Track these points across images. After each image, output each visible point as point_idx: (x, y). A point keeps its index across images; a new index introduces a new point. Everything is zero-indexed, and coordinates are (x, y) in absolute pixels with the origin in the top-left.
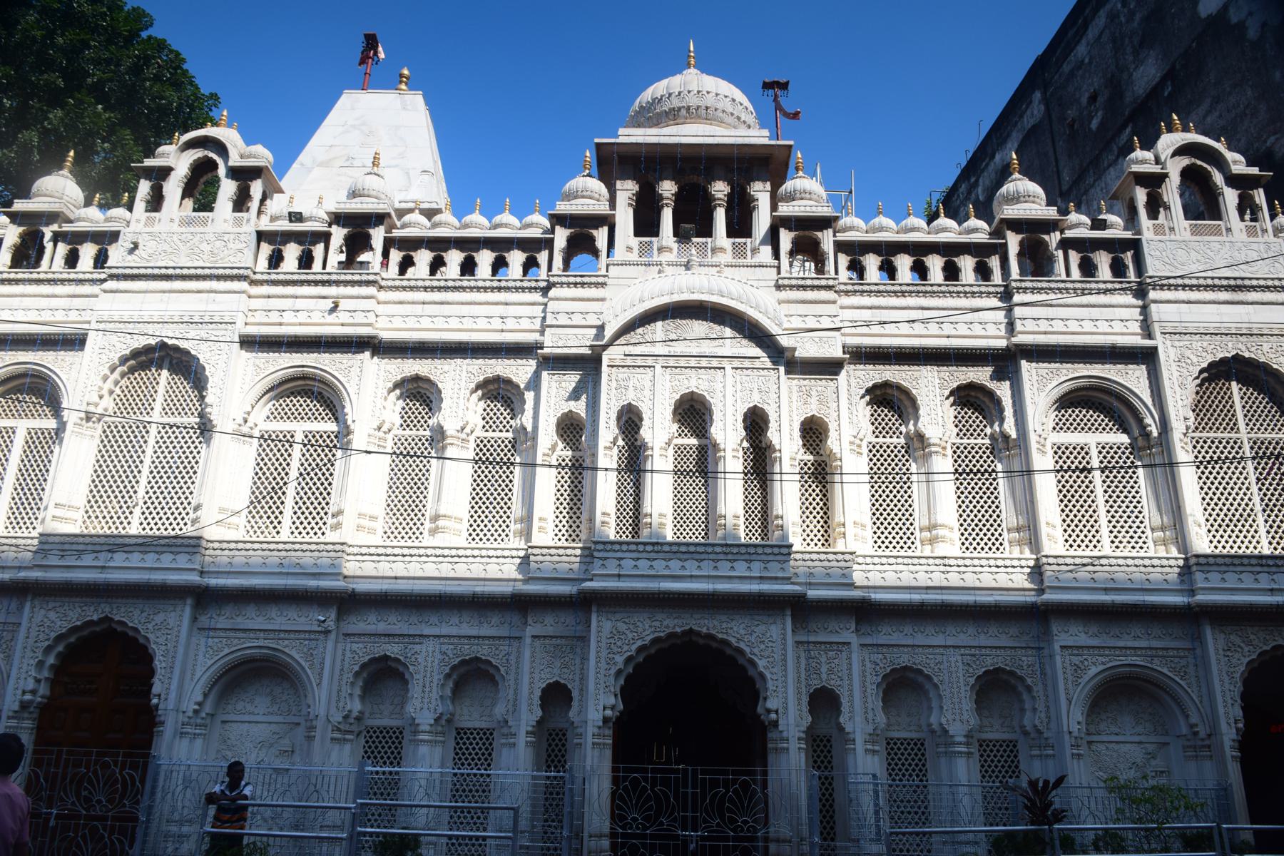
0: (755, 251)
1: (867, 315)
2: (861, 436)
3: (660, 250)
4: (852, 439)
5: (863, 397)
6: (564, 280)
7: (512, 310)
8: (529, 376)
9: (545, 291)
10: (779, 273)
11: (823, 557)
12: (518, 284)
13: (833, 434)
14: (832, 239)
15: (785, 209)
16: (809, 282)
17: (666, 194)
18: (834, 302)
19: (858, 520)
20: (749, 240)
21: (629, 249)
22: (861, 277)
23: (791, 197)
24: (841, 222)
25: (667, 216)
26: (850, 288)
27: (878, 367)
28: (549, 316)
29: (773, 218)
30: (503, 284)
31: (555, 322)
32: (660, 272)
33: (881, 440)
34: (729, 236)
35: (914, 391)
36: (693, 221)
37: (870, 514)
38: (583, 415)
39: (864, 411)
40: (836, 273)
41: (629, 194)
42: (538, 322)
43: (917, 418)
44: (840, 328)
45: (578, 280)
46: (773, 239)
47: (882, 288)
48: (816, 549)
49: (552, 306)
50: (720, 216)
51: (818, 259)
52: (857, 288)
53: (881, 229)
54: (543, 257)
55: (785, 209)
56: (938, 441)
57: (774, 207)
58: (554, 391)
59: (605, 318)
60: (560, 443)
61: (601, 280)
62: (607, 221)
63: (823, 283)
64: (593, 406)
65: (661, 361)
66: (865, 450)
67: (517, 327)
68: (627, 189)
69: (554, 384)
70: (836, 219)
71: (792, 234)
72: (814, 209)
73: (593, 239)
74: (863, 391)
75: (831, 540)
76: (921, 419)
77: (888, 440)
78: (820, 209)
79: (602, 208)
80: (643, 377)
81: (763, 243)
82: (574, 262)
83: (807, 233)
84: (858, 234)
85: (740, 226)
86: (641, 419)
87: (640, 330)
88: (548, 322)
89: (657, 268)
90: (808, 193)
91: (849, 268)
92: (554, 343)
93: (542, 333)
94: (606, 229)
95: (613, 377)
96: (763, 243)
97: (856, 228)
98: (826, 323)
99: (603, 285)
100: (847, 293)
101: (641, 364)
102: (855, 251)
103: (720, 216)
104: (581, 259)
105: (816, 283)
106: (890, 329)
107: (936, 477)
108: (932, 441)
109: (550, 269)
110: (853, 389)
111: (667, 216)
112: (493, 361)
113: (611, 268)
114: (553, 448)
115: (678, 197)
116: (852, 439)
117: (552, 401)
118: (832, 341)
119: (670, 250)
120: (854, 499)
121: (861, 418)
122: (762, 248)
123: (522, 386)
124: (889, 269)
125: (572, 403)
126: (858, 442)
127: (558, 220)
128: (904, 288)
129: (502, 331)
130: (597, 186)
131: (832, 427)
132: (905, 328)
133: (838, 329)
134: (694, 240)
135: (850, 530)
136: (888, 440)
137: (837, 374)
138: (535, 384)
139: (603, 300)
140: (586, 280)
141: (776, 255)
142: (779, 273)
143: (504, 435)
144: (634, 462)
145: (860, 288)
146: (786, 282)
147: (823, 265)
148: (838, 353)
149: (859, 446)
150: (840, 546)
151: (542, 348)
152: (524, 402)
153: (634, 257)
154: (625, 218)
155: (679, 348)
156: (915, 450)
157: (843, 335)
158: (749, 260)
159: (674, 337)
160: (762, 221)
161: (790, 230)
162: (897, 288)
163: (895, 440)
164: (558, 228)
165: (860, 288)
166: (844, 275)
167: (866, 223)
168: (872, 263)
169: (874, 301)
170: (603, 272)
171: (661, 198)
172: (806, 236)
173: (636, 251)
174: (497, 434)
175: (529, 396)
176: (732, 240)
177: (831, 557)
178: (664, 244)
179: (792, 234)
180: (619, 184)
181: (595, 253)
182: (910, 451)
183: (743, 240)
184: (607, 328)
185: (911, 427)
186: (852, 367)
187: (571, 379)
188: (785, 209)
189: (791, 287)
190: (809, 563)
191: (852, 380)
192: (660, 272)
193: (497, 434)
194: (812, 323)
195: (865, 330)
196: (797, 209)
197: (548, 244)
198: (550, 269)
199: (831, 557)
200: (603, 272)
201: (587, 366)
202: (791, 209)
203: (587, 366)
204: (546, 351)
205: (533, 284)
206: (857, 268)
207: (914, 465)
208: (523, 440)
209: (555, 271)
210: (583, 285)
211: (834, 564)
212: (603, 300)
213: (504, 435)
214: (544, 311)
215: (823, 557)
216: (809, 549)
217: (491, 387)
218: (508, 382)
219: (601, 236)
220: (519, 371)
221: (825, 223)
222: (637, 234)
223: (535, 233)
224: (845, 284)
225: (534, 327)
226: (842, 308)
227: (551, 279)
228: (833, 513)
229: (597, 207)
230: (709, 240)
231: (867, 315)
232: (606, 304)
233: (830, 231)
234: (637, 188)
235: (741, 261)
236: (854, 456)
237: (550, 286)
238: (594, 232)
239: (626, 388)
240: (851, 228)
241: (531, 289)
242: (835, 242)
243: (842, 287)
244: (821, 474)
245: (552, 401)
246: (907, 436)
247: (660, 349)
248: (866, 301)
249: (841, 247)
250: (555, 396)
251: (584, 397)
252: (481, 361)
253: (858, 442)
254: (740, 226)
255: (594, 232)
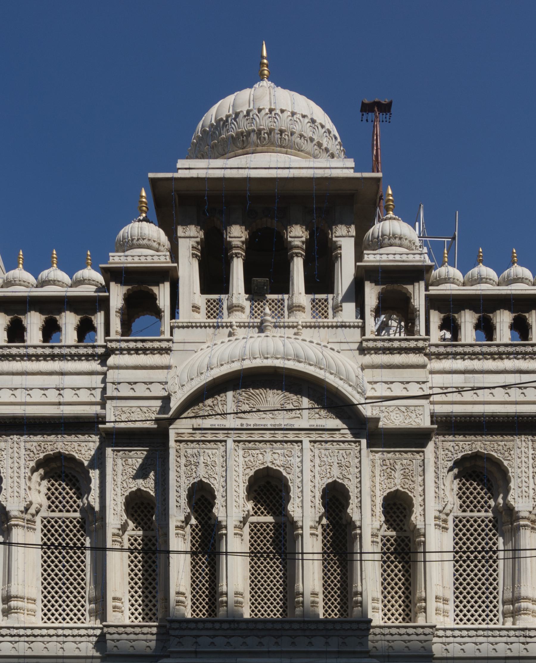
0: (337, 309)
1: (458, 380)
2: (447, 510)
3: (231, 309)
4: (437, 514)
5: (451, 469)
6: (124, 345)
7: (69, 381)
8: (92, 453)
9: (103, 359)
10: (363, 333)
11: (403, 631)
12: (73, 351)
13: (417, 510)
14: (423, 293)
15: (371, 257)
16: (396, 344)
17: (236, 242)
18: (424, 366)
19: (440, 594)
20: (330, 296)
21: (196, 308)
22: (455, 336)
23: (379, 243)
24: (435, 273)
25: (238, 268)
26: (442, 350)
27: (469, 438)
28: (109, 386)
29: (357, 268)
30: (57, 351)
31: (116, 394)
32: (230, 335)
33: (468, 514)
34: (308, 292)
35: (506, 463)
36: (268, 277)
37: (453, 589)
38: (152, 493)
39: (450, 487)
40: (428, 332)
41: (192, 242)
42: (98, 394)
43: (507, 491)
44: (430, 395)
45: (140, 345)
46: (357, 294)
47: (477, 349)
48: (397, 623)
49: (112, 375)
50: (298, 268)
51: (408, 316)
52: (449, 349)
53: (480, 280)
54: (99, 319)
55: (371, 257)
56: (527, 514)
57: (359, 257)
58: (120, 468)
59: (170, 387)
60: (130, 522)
61: (164, 345)
62: (170, 276)
63: (412, 344)
64: (162, 484)
65: (234, 436)
66: (451, 525)
67: (75, 399)
68: (190, 237)
69: (119, 462)
70: (429, 269)
71: (378, 289)
72: (404, 257)
73: (153, 298)
74: (450, 464)
75: (412, 615)
76: (512, 492)
77: (476, 514)
78: (411, 257)
79: (162, 260)
80: (214, 454)
81: (346, 299)
82: (137, 324)
83: (396, 287)
84: (454, 286)
85: (320, 280)
86: (214, 497)
87: (209, 402)
88: (109, 393)
89: (226, 331)
90: (401, 238)
91: (441, 328)
92: (115, 416)
93: (103, 405)
94: (167, 285)
95: (182, 453)
96: (346, 299)
97: (452, 279)
98: (414, 390)
99: (168, 351)
100: (439, 356)
101: (214, 438)
102: (449, 307)
103: (298, 268)
104: (142, 321)
105: (404, 344)
106: (484, 395)
107: (523, 554)
108: (522, 514)
109: (107, 332)
110: (440, 461)
111: (238, 268)
112: (52, 438)
113: (176, 331)
114: (124, 528)
115: (250, 246)
116: (437, 514)
117: (119, 479)
118: (419, 411)
119: (242, 309)
120: (438, 576)
121: (447, 493)
122: (344, 305)
123: (86, 463)
124: (486, 328)
125: (140, 481)
126: (443, 516)
127: (113, 275)
128: (502, 349)
129: (60, 404)
130: (154, 232)
131: (417, 501)
132: (500, 395)
133: (426, 397)
134: (269, 296)
135: (432, 605)
136: (476, 514)
137: (424, 445)
138: (99, 461)
139: (168, 367)
140: (148, 345)
141: (361, 312)
142: (363, 333)
143: (72, 515)
144: (208, 543)
145: (454, 349)
146: (371, 344)
147: (413, 324)
148: (426, 423)
149: (445, 521)
150: (421, 621)
151: (104, 423)
152: (89, 480)
153: (201, 317)
154: (189, 272)
155: (252, 420)
156: (503, 524)
157: (432, 403)
158: (330, 320)
159: (246, 408)
160: (346, 273)
161: (377, 284)
162: (494, 349)
163: (483, 514)
164: (112, 285)
165: (454, 349)
166: (436, 335)
167: (464, 273)
168: (468, 320)
169: (468, 364)
170: (167, 336)
171: (230, 246)
172: (394, 288)
173: (203, 310)
174: (65, 514)
175: (94, 474)
176: (311, 296)
177: (411, 631)
178: (235, 301)
179: (378, 289)
180: (180, 231)
181: (158, 313)
182: (498, 526)
183: (324, 296)
184: (172, 399)
185: (500, 501)
186: (441, 438)
187: (137, 457)
188: (372, 258)
189: (377, 350)
190: (389, 637)
191: (441, 452)
192: (230, 335)
193: (65, 514)
194: (398, 390)
195: (456, 397)
196: (384, 257)
197: (102, 304)
198: (107, 332)
199: (411, 631)
200: (167, 336)
201: (152, 443)
202: (378, 257)
203: (152, 443)
204: (108, 425)
205: (90, 351)
206: (451, 325)
207: (501, 540)
208: (93, 521)
209: (113, 336)
210: (145, 351)
211: (414, 637)
212: (168, 367)
213: (72, 515)
214: (104, 381)
215: (403, 631)
216: (389, 623)
217: (53, 465)
218: (71, 459)
219: (163, 294)
220: (83, 448)
221: (417, 274)
222: (204, 290)
223: (88, 290)
224: (437, 346)
225: (93, 400)
226: (432, 372)
227: (109, 345)
228: (415, 590)
229: (156, 259)
230: (286, 296)
231: (458, 380)
232: (172, 372)
233: (422, 284)
234: (201, 234)
235: (321, 321)
236: (438, 532)
237: (109, 352)
238: (155, 289)
239: (197, 464)
240: (447, 280)
241: (88, 357)
242: (427, 296)
243: (433, 349)
244: (405, 551)
245: (119, 479)
246: (496, 510)
247: (231, 422)
248: (459, 364)
249: (433, 302)
250: (119, 478)
251: (152, 474)
252: (39, 438)
253: (443, 516)
254: (320, 280)
255: (155, 289)
